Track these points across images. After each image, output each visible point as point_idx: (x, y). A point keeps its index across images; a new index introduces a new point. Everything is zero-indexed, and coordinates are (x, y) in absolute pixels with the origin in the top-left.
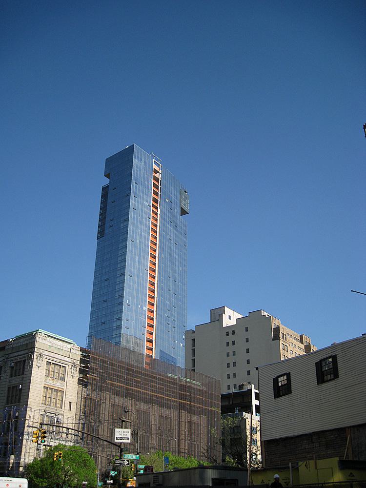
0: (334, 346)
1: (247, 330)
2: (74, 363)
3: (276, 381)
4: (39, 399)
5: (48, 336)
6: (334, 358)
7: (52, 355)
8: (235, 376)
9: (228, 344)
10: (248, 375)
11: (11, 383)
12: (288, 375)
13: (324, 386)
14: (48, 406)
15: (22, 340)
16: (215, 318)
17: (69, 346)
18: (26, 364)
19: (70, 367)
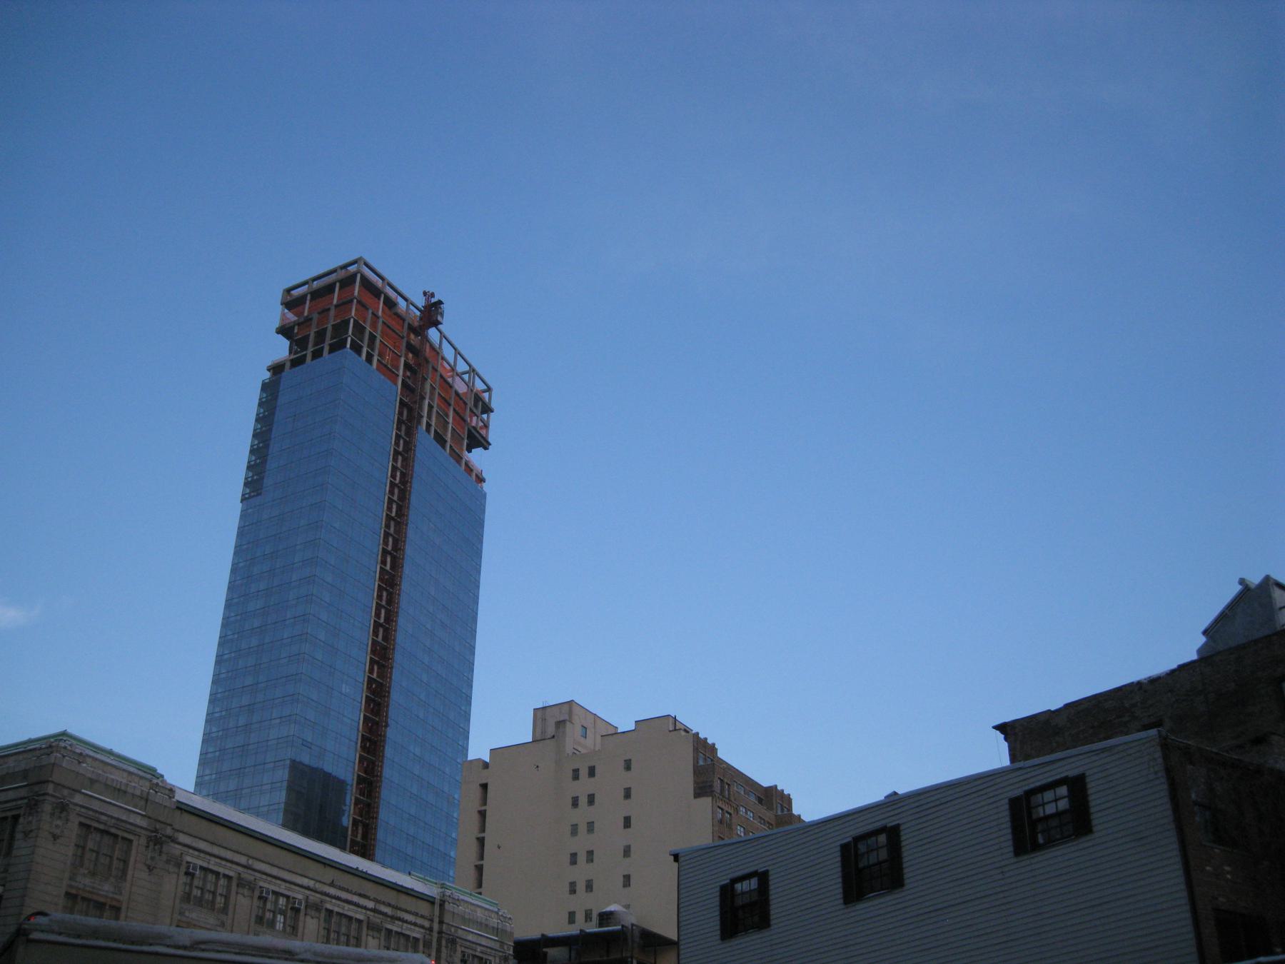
0: (894, 800)
1: (628, 766)
2: (156, 831)
3: (727, 892)
6: (893, 833)
9: (575, 802)
10: (625, 886)
12: (763, 877)
13: (863, 909)
16: (543, 732)
18: (20, 828)
19: (143, 841)
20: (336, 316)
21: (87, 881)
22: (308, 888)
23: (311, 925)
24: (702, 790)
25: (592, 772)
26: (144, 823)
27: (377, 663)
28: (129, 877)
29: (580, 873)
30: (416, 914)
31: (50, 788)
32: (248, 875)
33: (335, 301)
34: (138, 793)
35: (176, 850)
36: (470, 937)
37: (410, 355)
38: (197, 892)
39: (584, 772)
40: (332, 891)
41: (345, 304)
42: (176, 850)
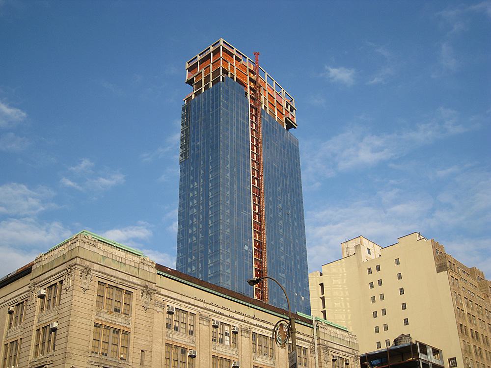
1: (398, 262)
2: (146, 287)
4: (86, 343)
5: (98, 240)
7: (108, 271)
8: (386, 328)
9: (372, 285)
11: (41, 323)
14: (103, 357)
15: (56, 252)
17: (137, 259)
18: (64, 287)
20: (213, 68)
21: (107, 316)
22: (242, 321)
23: (245, 341)
24: (441, 268)
25: (378, 269)
26: (139, 282)
27: (258, 232)
28: (133, 314)
29: (380, 321)
30: (303, 334)
31: (78, 261)
32: (205, 313)
33: (212, 62)
34: (133, 264)
35: (160, 298)
36: (336, 347)
37: (252, 84)
38: (174, 324)
39: (374, 269)
40: (255, 322)
41: (216, 62)
42: (160, 298)
